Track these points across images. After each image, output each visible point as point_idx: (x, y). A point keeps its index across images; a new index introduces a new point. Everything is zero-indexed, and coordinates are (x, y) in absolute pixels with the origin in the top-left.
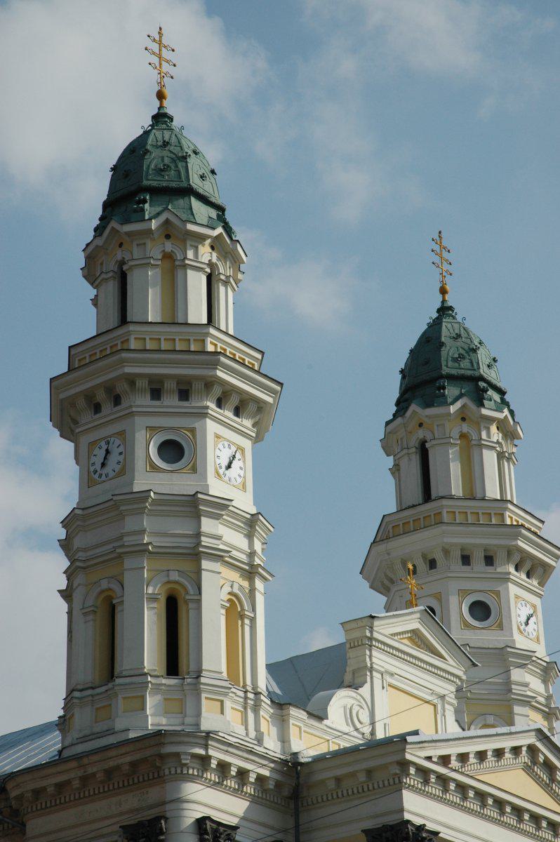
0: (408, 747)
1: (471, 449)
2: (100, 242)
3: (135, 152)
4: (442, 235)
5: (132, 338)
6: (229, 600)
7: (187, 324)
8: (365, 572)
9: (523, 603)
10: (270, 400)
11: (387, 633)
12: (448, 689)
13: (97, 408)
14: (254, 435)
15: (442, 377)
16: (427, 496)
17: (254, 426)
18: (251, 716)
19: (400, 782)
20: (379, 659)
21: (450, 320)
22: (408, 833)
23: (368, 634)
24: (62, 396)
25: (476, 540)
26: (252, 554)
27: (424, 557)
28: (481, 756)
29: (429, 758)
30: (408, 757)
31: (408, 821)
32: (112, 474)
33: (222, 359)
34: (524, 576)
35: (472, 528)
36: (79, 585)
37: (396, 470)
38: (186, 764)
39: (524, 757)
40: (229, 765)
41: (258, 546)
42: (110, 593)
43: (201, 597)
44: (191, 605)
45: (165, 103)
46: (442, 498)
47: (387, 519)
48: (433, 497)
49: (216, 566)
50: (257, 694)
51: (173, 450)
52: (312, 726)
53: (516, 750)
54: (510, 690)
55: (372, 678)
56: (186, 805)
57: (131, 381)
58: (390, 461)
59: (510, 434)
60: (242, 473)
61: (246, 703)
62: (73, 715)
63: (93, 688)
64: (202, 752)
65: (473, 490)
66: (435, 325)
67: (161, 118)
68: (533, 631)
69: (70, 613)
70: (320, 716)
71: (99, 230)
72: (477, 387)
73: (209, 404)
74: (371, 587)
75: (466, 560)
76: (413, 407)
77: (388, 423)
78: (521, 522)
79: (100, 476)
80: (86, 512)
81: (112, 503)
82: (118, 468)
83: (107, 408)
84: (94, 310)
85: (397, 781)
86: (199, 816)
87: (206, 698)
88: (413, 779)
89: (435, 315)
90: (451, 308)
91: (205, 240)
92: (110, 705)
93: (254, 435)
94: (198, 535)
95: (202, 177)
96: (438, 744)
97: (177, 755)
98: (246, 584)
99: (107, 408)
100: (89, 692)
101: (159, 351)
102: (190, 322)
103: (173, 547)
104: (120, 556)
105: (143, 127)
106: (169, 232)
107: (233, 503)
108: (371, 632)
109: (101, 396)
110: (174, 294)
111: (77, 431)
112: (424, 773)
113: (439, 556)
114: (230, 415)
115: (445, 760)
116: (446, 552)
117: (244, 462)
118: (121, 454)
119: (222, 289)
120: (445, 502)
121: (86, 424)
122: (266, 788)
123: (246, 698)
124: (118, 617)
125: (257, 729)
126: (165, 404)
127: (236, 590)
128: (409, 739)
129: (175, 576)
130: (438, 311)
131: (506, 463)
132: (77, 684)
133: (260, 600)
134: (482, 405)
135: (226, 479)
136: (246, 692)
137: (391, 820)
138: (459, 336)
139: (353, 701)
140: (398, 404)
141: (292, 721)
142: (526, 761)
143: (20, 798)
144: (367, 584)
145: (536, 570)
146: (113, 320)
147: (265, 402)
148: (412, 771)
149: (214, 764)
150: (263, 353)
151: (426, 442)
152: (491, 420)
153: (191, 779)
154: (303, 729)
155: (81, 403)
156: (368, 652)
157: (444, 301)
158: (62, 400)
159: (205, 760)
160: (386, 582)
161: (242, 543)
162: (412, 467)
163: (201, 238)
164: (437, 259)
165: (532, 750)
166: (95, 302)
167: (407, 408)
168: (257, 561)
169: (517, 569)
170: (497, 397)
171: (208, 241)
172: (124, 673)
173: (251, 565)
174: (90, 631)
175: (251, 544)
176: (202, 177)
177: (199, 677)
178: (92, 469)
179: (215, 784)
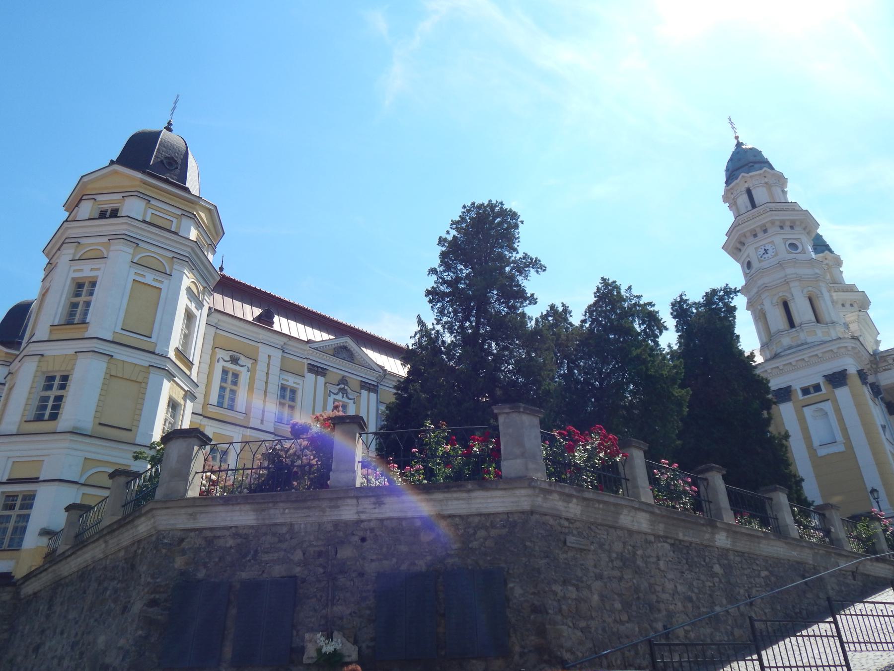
45: (739, 139)
57: (773, 222)
67: (739, 145)
82: (773, 254)
83: (761, 235)
129: (810, 289)
155: (748, 234)
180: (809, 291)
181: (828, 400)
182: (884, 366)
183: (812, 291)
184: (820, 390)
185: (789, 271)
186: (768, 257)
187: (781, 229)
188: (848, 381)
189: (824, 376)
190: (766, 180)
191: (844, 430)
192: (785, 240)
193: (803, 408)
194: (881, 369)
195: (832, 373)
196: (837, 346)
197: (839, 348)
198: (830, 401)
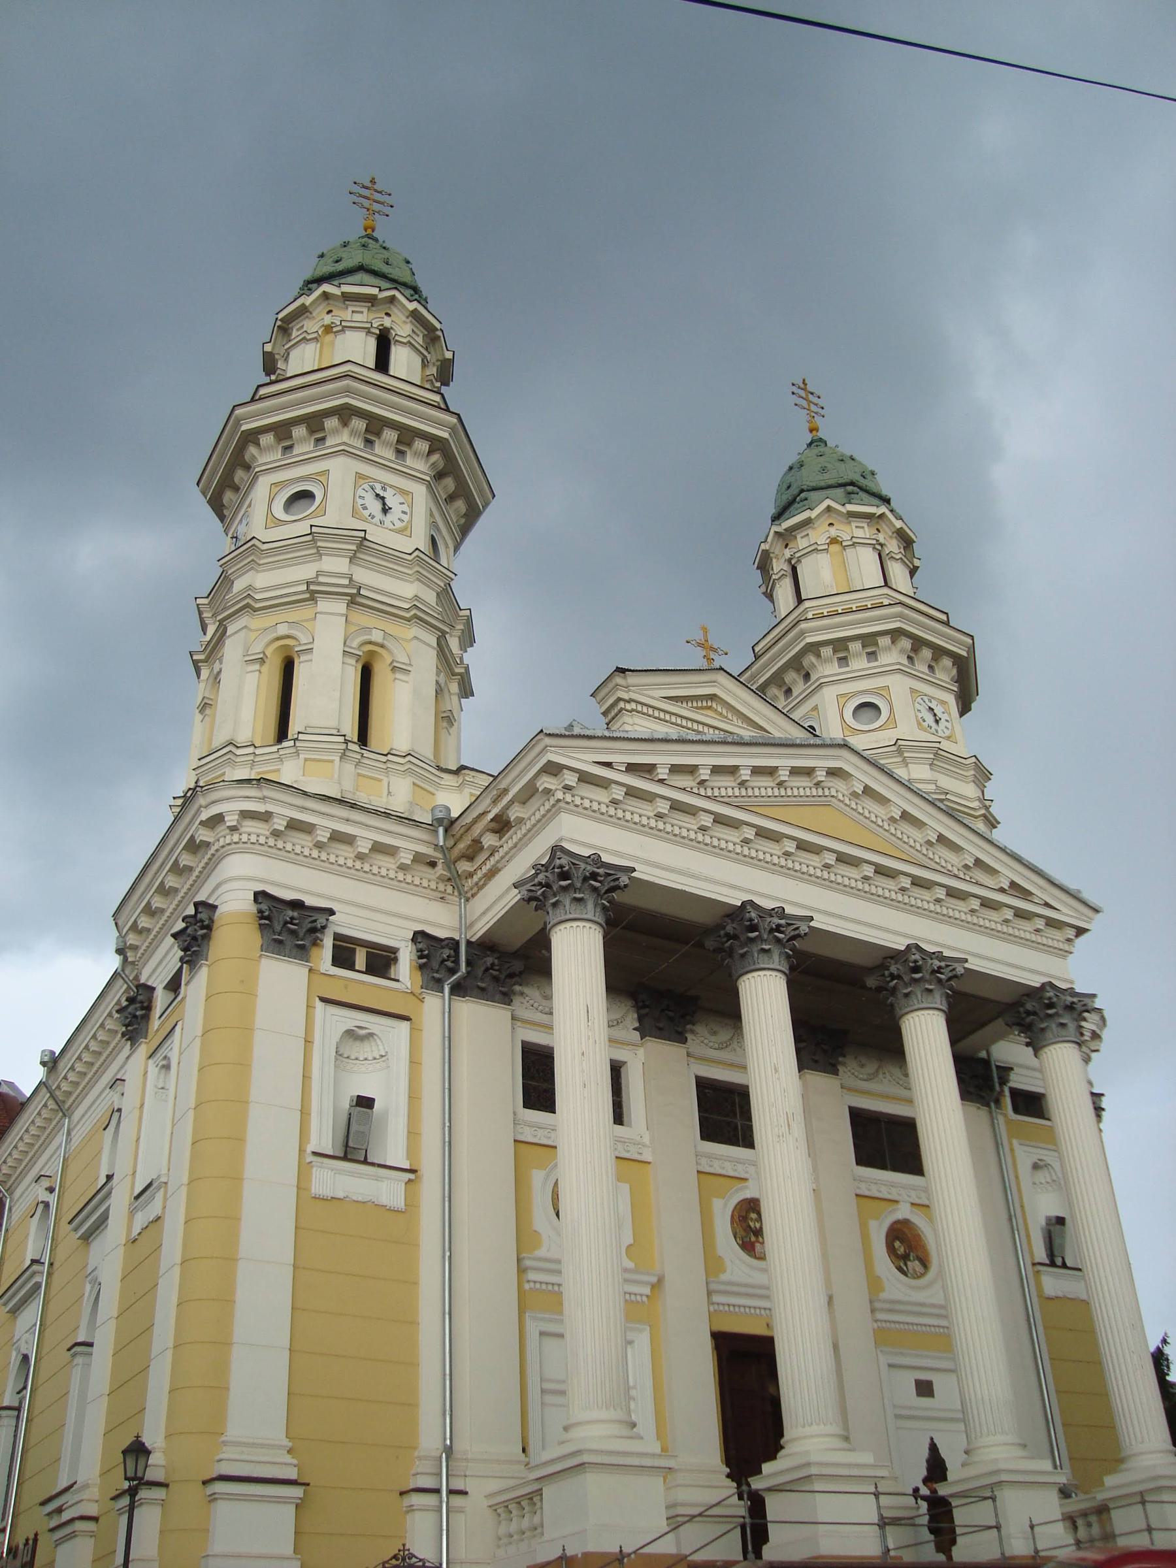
4: (806, 382)
9: (925, 698)
10: (445, 435)
29: (608, 765)
38: (233, 829)
60: (406, 518)
68: (945, 730)
87: (306, 760)
90: (821, 440)
117: (411, 507)
129: (283, 630)
134: (850, 503)
135: (376, 520)
142: (833, 793)
162: (784, 593)
164: (804, 403)
165: (832, 773)
183: (288, 637)
198: (178, 1028)
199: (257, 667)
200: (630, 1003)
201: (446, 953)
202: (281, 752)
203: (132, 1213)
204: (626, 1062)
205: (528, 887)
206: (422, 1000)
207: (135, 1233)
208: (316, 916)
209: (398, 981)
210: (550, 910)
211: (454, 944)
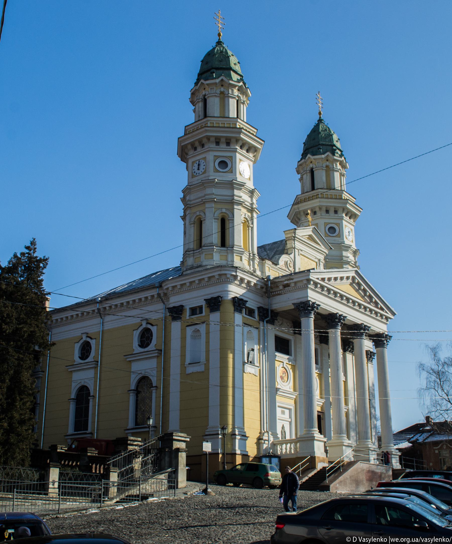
0: (311, 274)
1: (329, 171)
2: (197, 87)
3: (211, 54)
5: (209, 122)
6: (244, 220)
7: (229, 118)
8: (289, 217)
11: (301, 235)
12: (322, 257)
13: (195, 149)
14: (253, 160)
15: (319, 144)
16: (313, 188)
17: (254, 156)
18: (251, 262)
19: (307, 287)
20: (298, 245)
21: (323, 124)
22: (310, 305)
23: (294, 235)
24: (182, 144)
25: (332, 203)
26: (252, 204)
27: (312, 211)
28: (336, 279)
29: (318, 279)
30: (311, 278)
31: (310, 301)
32: (201, 173)
33: (243, 131)
34: (348, 218)
35: (330, 200)
36: (189, 213)
37: (301, 179)
38: (229, 278)
39: (350, 281)
40: (244, 279)
41: (254, 201)
42: (200, 216)
43: (234, 217)
44: (230, 221)
46: (319, 189)
47: (298, 197)
48: (315, 189)
49: (240, 207)
50: (254, 255)
51: (223, 164)
52: (273, 267)
53: (348, 278)
54: (342, 259)
55: (295, 251)
56: (229, 293)
57: (208, 138)
58: (299, 176)
59: (344, 167)
61: (250, 258)
62: (186, 260)
63: (193, 251)
64: (234, 274)
65: (331, 187)
66: (317, 126)
69: (185, 225)
70: (276, 264)
71: (196, 84)
72: (332, 149)
73: (237, 147)
74: (291, 222)
75: (327, 212)
76: (309, 155)
77: (299, 162)
78: (348, 198)
79: (197, 174)
80: (191, 187)
81: (201, 183)
82: (203, 171)
83: (199, 149)
84: (194, 114)
85: (306, 286)
86: (233, 296)
88: (311, 286)
89: (317, 122)
91: (236, 87)
92: (200, 257)
93: (253, 160)
94: (233, 195)
95: (235, 64)
96: (321, 273)
97: (226, 274)
98: (250, 214)
99: (199, 149)
100: (192, 252)
101: (219, 127)
102: (230, 117)
103: (224, 200)
104: (204, 203)
105: (213, 46)
106: (222, 84)
107: (246, 184)
108: (295, 235)
109: (197, 144)
110: (224, 106)
111: (188, 157)
112: (316, 284)
113: (317, 210)
114: (245, 152)
115: (323, 279)
116: (320, 209)
118: (204, 165)
119: (242, 105)
120: (320, 190)
121: (191, 155)
122: (257, 288)
123: (250, 256)
124: (203, 225)
125: (254, 267)
126: (221, 147)
127: (247, 217)
128: (311, 271)
129: (224, 210)
130: (318, 121)
131: (342, 177)
132: (188, 249)
133: (255, 221)
136: (250, 254)
137: (303, 300)
138: (326, 130)
139: (288, 259)
140: (302, 155)
141: (266, 265)
143: (167, 289)
144: (290, 221)
145: (353, 216)
146: (202, 114)
147: (258, 148)
148: (312, 283)
149: (239, 278)
150: (257, 130)
151: (313, 168)
152: (337, 161)
153: (230, 283)
154: (270, 268)
155: (189, 147)
156: (293, 242)
157: (320, 117)
158: (182, 146)
159: (235, 277)
160: (297, 220)
161: (249, 199)
162: (307, 178)
163: (235, 86)
166: (194, 111)
167: (306, 156)
168: (254, 206)
169: (346, 215)
170: (339, 153)
171: (237, 88)
172: (205, 245)
173: (252, 208)
174: (192, 231)
175: (252, 200)
176: (235, 64)
177: (233, 247)
178: (193, 171)
179: (239, 285)
180: (222, 213)
181: (204, 322)
182: (277, 291)
183: (225, 213)
184: (201, 312)
185: (208, 191)
186: (199, 173)
187: (216, 145)
188: (221, 308)
189: (205, 300)
190: (222, 89)
191: (208, 351)
192: (216, 157)
193: (187, 328)
194: (275, 293)
195: (210, 298)
196: (219, 273)
197: (220, 275)
199: (217, 221)
200: (292, 324)
201: (265, 312)
202: (228, 251)
203: (183, 366)
204: (291, 340)
205: (296, 305)
206: (259, 323)
207: (187, 373)
208: (244, 302)
209: (255, 318)
210: (303, 313)
211: (267, 310)
